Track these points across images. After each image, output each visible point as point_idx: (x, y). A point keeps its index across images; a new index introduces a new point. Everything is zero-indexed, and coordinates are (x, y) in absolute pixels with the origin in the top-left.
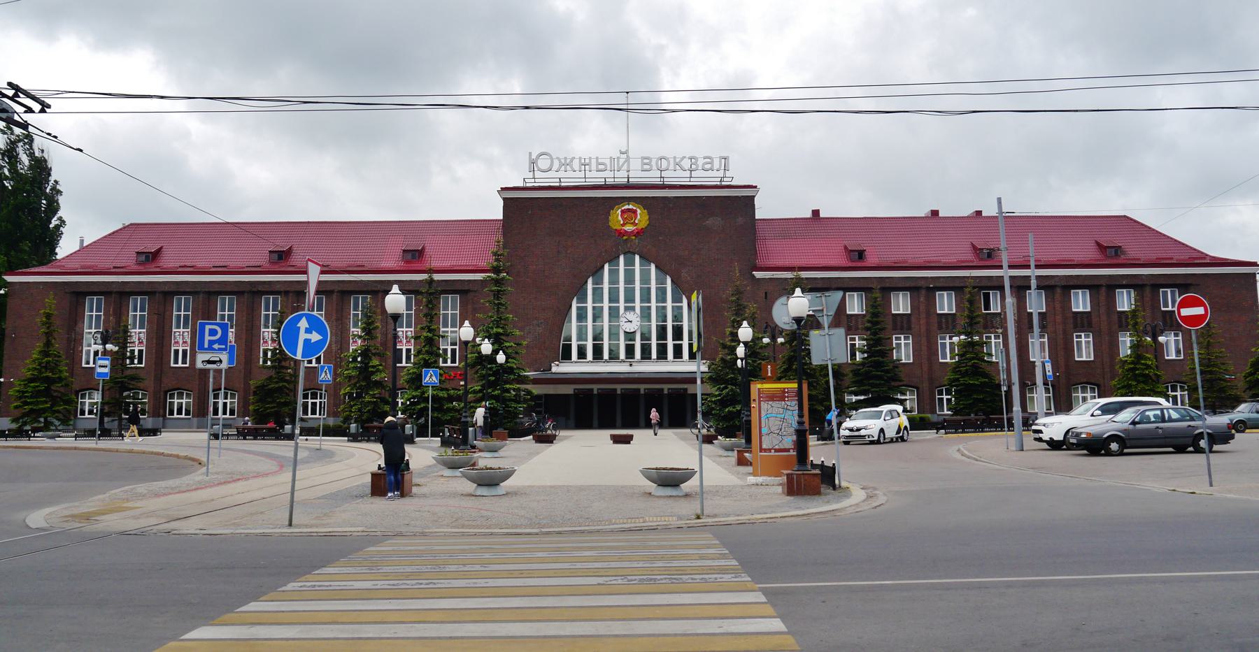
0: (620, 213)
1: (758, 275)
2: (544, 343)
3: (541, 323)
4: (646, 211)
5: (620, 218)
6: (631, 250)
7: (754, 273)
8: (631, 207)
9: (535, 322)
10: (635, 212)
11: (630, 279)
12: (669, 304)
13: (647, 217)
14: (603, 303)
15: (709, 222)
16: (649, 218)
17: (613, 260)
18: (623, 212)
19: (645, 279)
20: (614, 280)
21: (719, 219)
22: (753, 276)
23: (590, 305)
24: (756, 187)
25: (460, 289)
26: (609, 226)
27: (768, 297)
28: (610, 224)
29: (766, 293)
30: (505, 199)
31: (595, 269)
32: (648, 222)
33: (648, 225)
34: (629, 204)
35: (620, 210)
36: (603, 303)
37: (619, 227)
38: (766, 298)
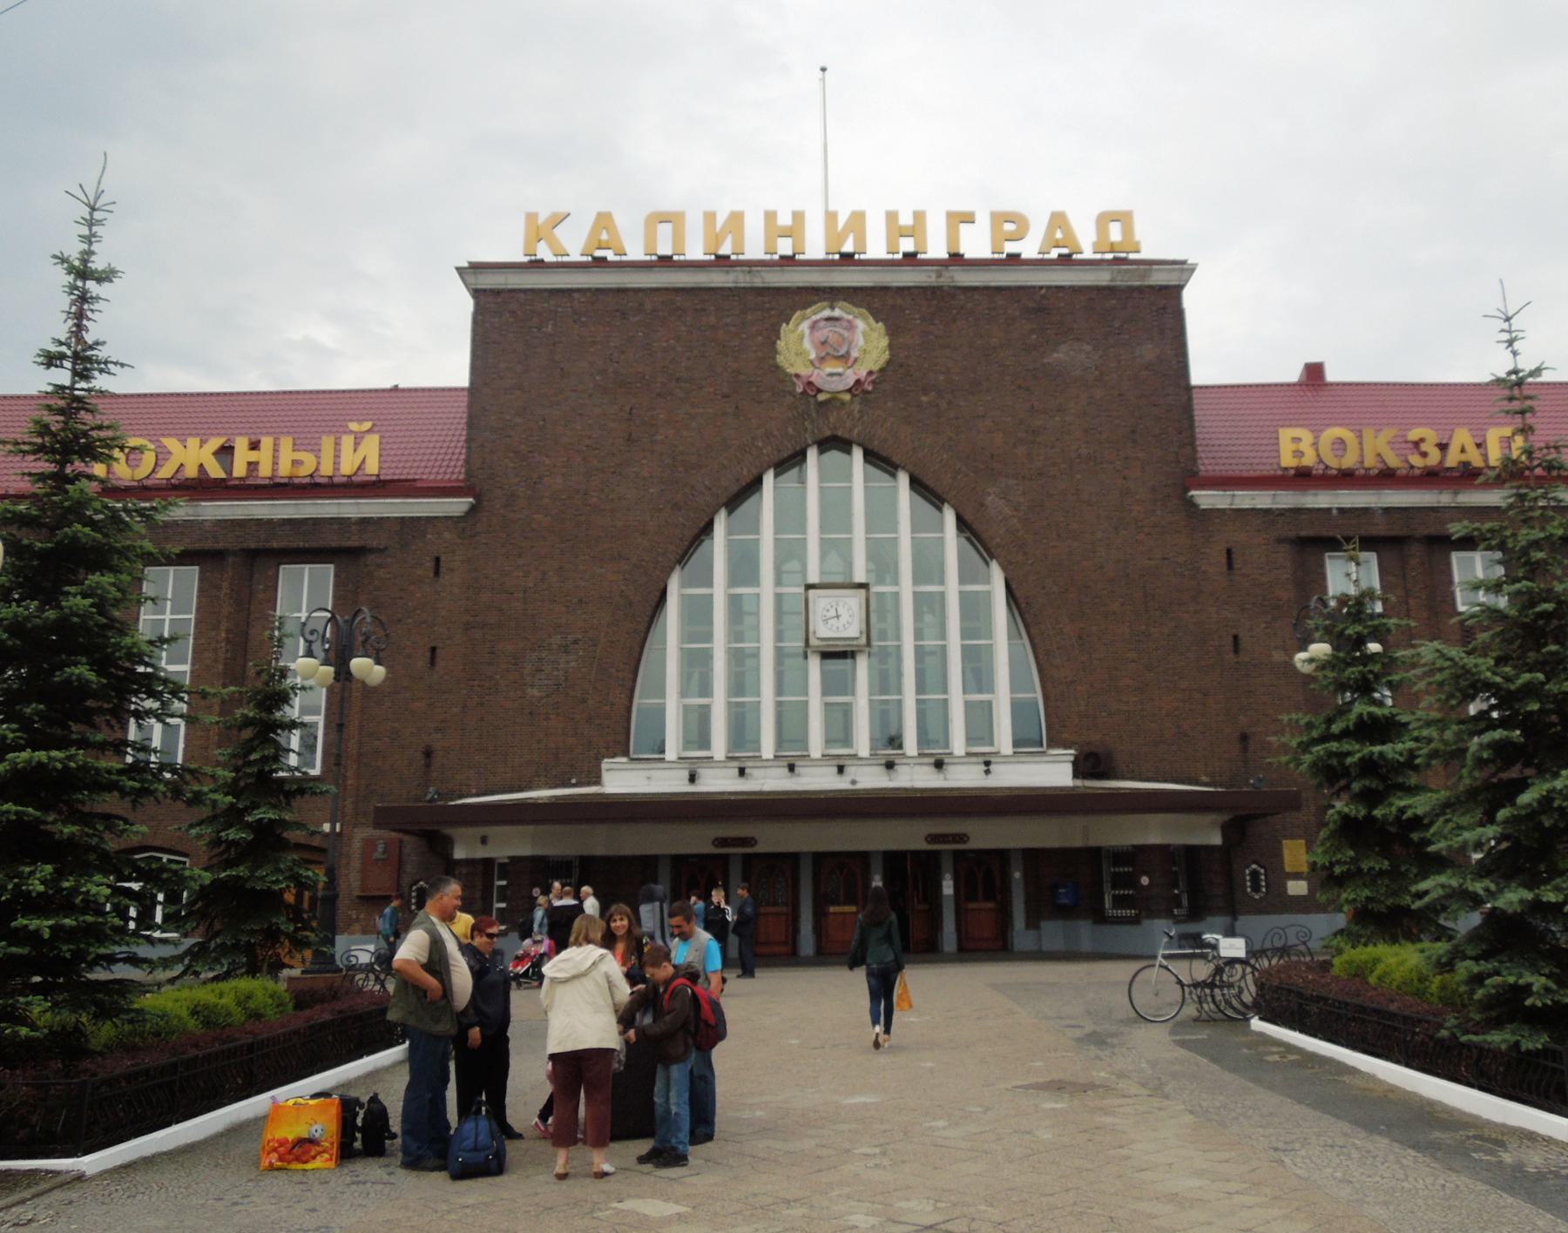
0: (807, 332)
1: (1206, 498)
2: (584, 701)
3: (576, 642)
4: (880, 324)
5: (807, 344)
6: (840, 434)
7: (1193, 493)
8: (837, 313)
9: (556, 640)
10: (851, 327)
11: (836, 513)
12: (952, 588)
13: (885, 342)
14: (758, 586)
15: (1060, 355)
16: (890, 346)
17: (791, 461)
18: (813, 327)
19: (881, 517)
20: (790, 518)
21: (1088, 348)
22: (1191, 504)
23: (719, 591)
24: (1183, 262)
25: (334, 544)
26: (777, 368)
27: (1237, 564)
28: (780, 359)
29: (1229, 552)
30: (477, 293)
31: (734, 489)
32: (886, 356)
33: (889, 363)
34: (832, 308)
35: (805, 326)
36: (758, 586)
37: (804, 371)
38: (1230, 565)
